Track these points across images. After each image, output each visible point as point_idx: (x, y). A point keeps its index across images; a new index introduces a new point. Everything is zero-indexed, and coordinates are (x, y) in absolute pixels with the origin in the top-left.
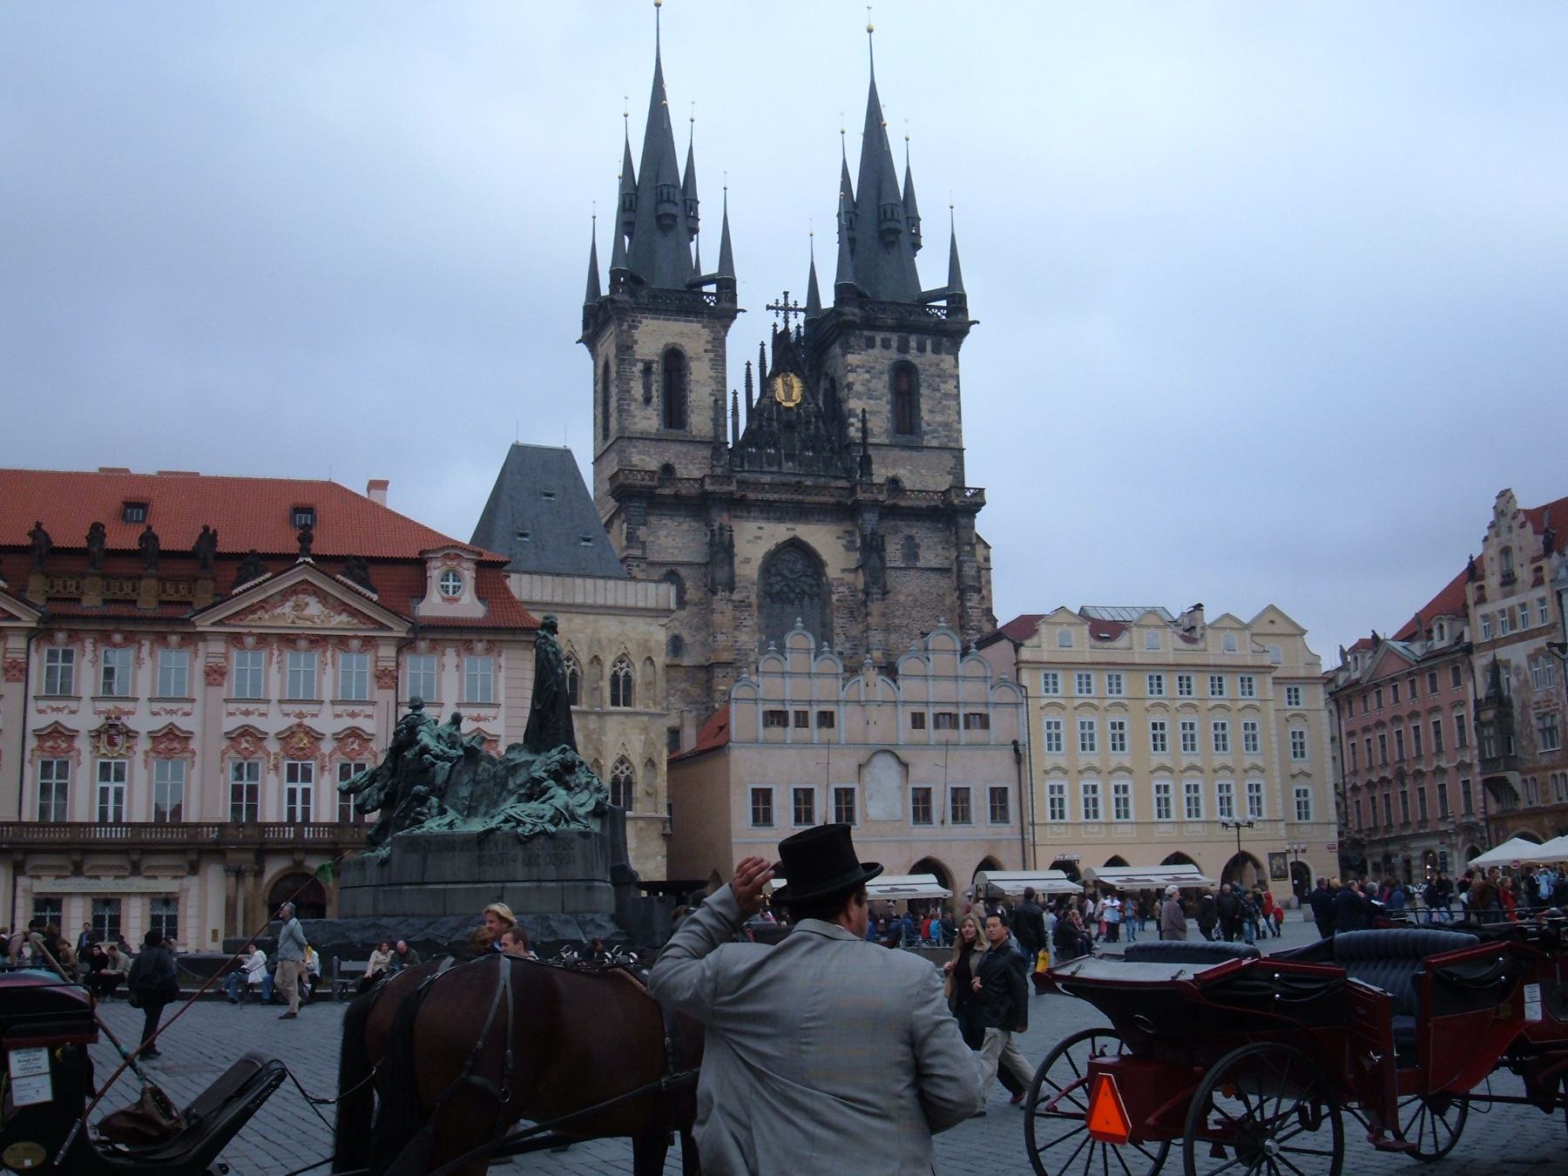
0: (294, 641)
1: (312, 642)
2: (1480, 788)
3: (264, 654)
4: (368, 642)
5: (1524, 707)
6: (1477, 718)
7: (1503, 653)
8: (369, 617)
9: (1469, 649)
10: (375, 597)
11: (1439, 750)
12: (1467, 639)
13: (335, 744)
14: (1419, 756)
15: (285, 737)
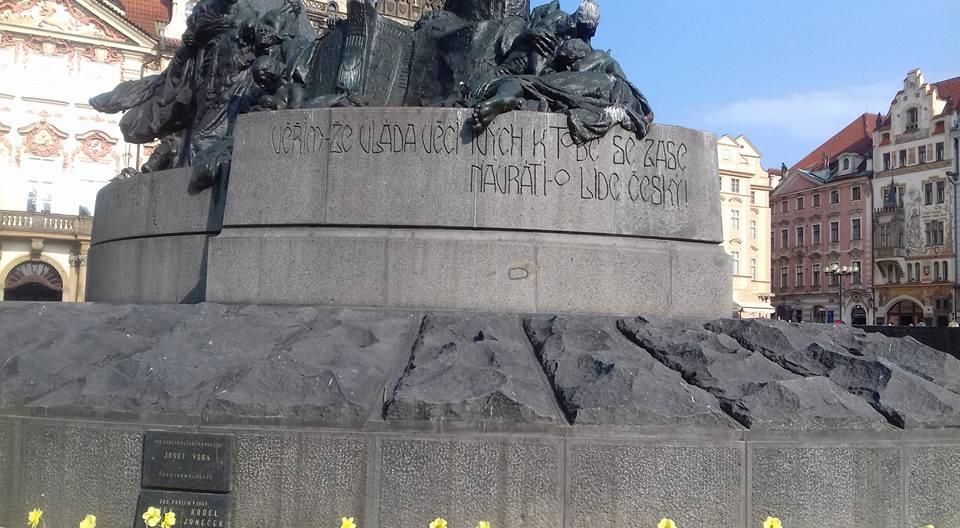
0: (40, 43)
1: (58, 46)
2: (869, 267)
3: (12, 50)
4: (115, 53)
5: (915, 216)
6: (874, 221)
7: (899, 179)
8: (116, 31)
9: (871, 175)
10: (123, 13)
11: (835, 241)
12: (868, 168)
13: (79, 144)
14: (817, 245)
15: (28, 133)
